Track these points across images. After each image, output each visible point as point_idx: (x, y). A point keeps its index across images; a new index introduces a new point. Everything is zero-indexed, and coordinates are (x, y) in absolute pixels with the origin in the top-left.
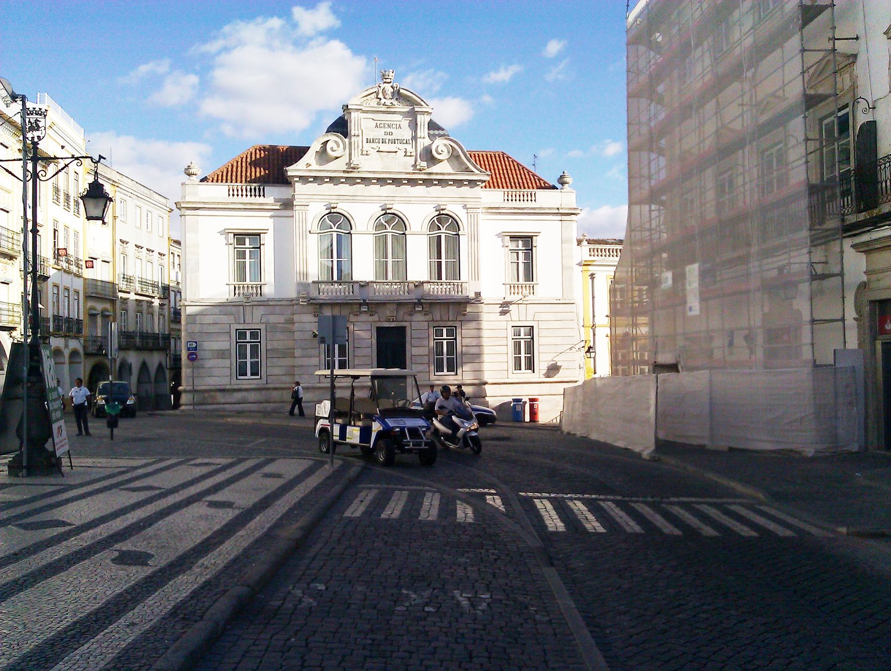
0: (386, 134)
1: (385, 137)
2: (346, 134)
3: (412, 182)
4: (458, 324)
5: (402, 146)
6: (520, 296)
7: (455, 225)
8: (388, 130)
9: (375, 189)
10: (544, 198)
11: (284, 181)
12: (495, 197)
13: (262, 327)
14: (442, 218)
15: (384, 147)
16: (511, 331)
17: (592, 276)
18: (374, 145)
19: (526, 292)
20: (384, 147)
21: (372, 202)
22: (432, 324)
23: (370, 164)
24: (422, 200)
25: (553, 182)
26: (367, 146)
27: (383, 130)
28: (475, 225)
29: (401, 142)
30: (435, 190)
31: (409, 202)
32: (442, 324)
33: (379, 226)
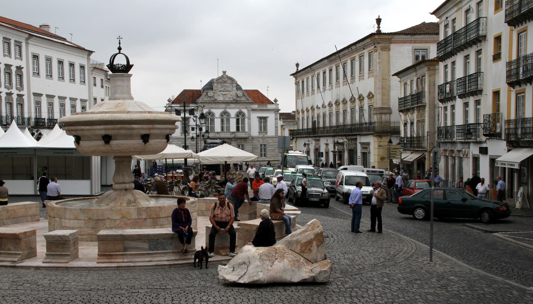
0: (224, 89)
1: (224, 90)
2: (212, 89)
3: (232, 103)
4: (244, 144)
5: (229, 93)
6: (262, 135)
7: (244, 115)
8: (224, 88)
9: (221, 106)
10: (270, 107)
11: (194, 102)
12: (255, 106)
13: (189, 145)
14: (240, 114)
15: (224, 93)
16: (259, 145)
17: (284, 129)
18: (221, 92)
19: (264, 134)
20: (224, 93)
21: (220, 109)
22: (237, 144)
23: (221, 98)
24: (234, 108)
25: (272, 100)
26: (219, 93)
27: (223, 88)
28: (249, 115)
29: (228, 91)
30: (238, 106)
31: (230, 109)
32: (240, 144)
33: (222, 116)
